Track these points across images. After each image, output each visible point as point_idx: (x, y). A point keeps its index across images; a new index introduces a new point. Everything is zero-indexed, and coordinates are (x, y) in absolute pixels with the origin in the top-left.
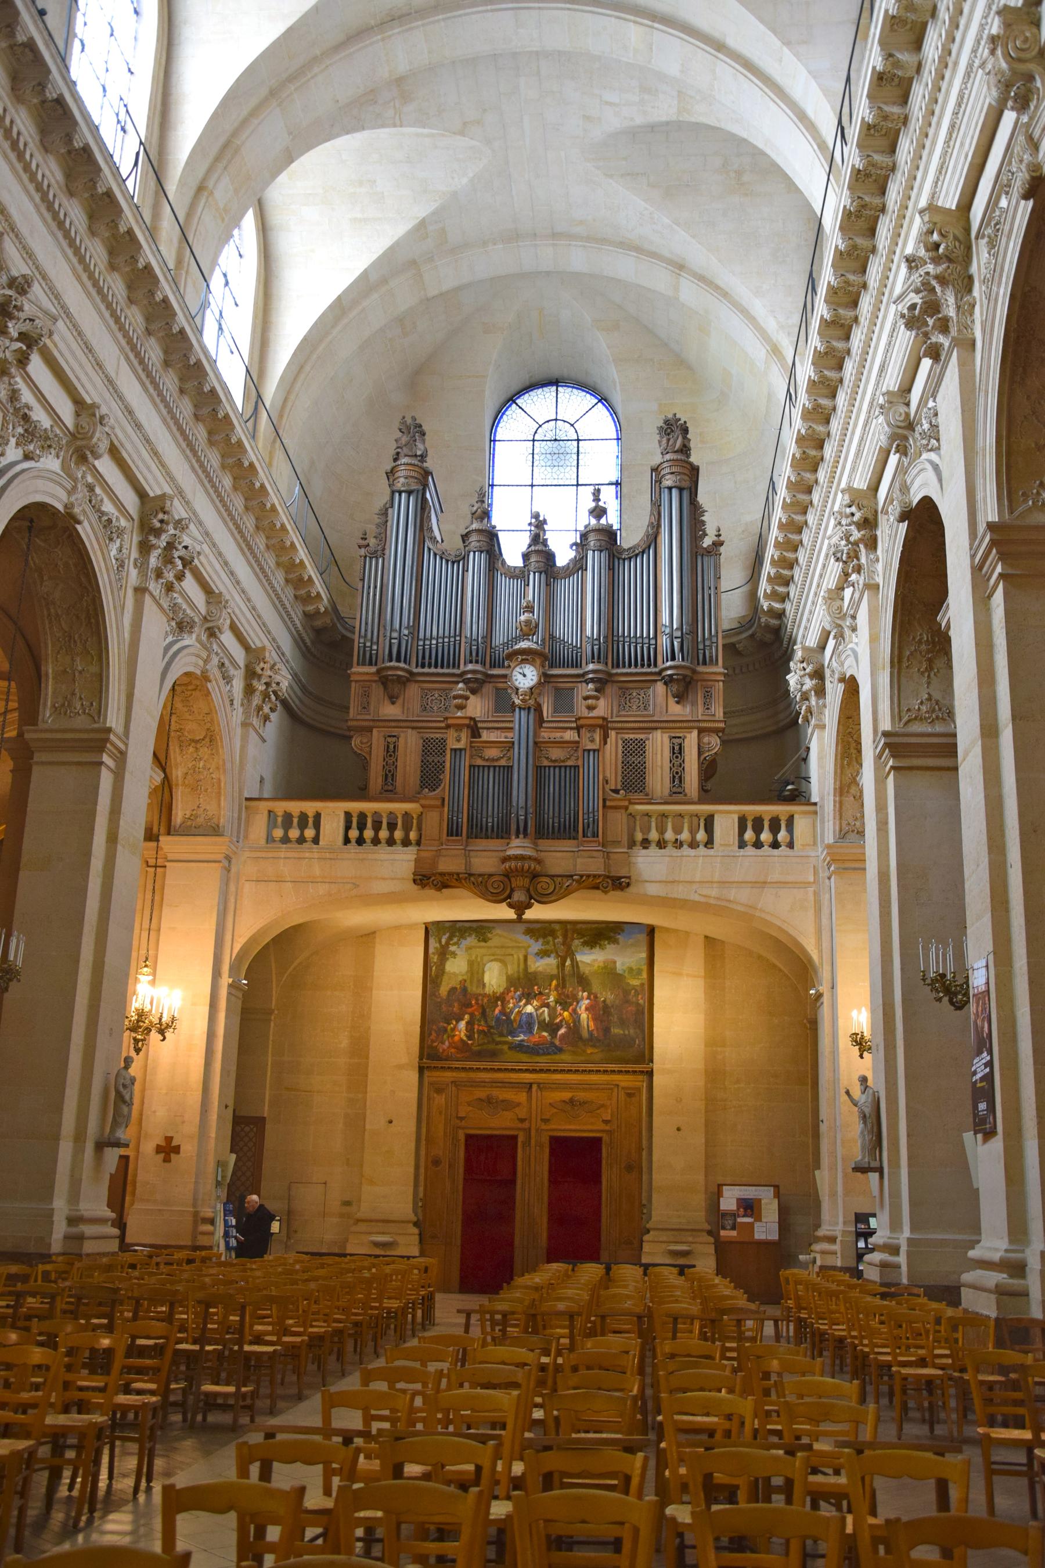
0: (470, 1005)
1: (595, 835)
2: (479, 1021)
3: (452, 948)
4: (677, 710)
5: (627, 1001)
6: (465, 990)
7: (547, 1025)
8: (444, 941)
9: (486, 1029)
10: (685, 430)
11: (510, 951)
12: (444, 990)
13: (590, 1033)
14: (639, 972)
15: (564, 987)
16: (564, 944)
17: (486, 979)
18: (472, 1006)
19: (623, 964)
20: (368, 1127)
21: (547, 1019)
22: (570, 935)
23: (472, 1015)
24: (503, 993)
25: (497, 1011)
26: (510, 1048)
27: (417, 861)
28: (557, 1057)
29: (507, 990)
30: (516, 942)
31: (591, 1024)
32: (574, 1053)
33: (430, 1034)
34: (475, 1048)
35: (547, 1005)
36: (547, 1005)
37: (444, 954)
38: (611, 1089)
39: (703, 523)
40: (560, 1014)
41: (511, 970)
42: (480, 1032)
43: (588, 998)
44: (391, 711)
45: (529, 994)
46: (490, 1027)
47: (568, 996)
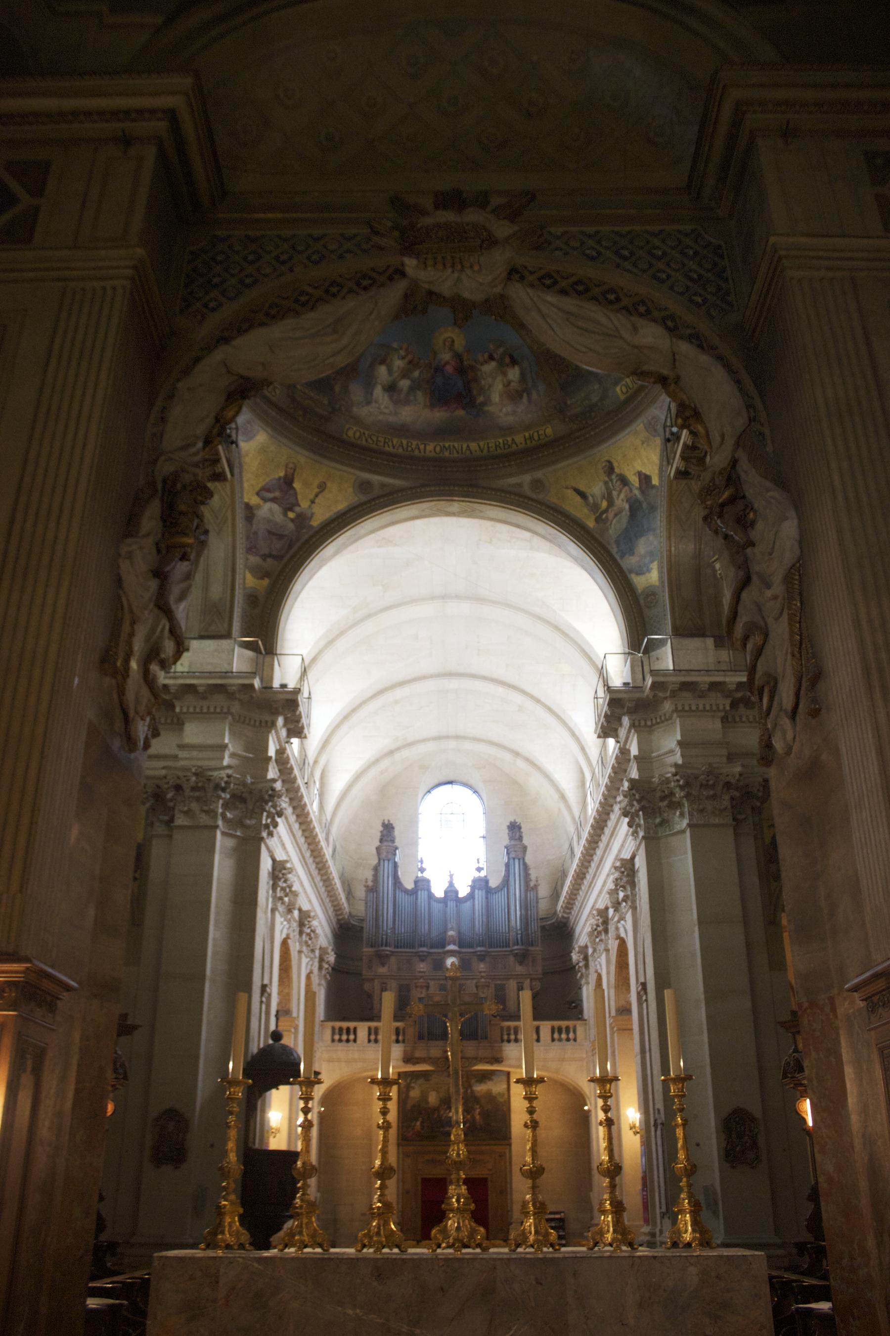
1: (486, 1038)
3: (413, 1085)
4: (520, 969)
10: (520, 828)
25: (435, 1116)
27: (405, 1052)
37: (408, 1088)
39: (529, 874)
44: (383, 970)
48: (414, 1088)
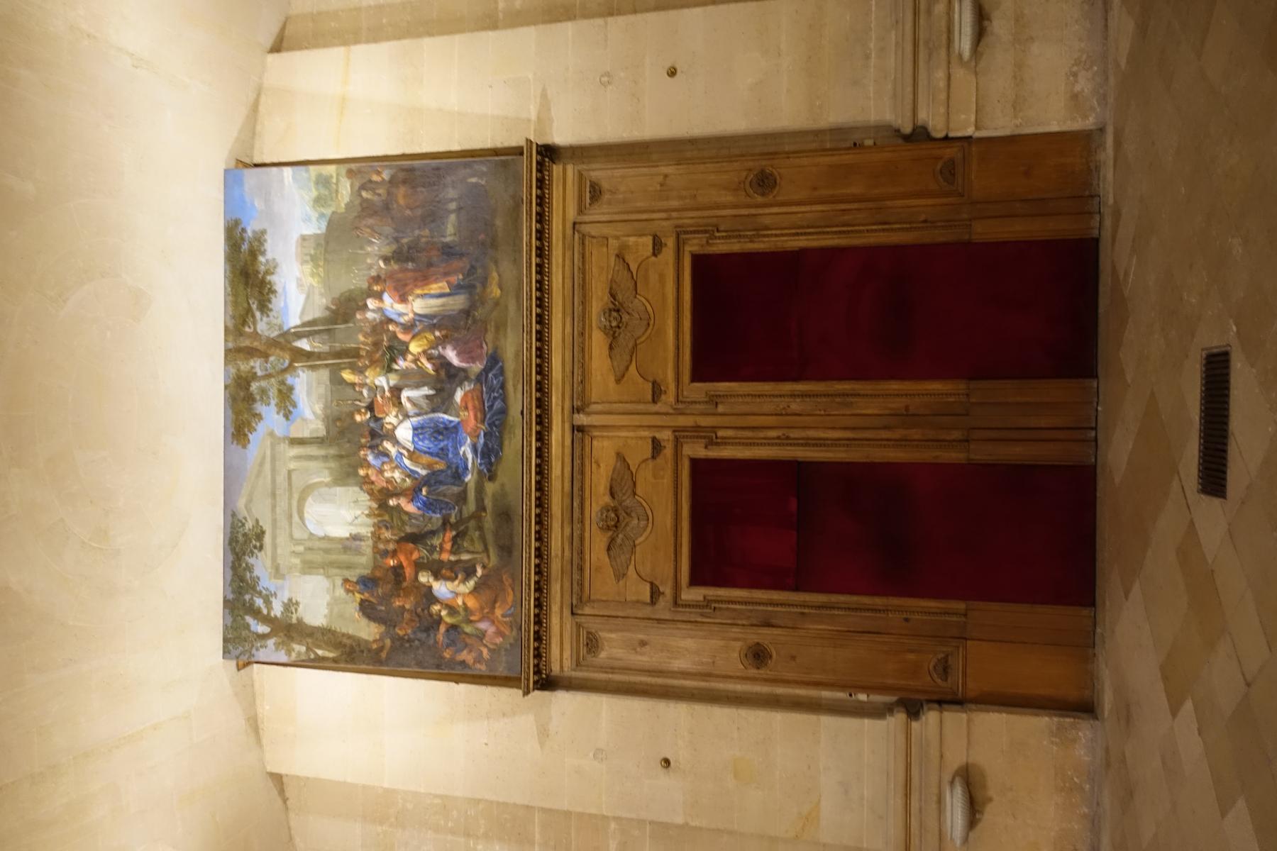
0: (398, 571)
2: (432, 549)
3: (277, 610)
5: (387, 207)
6: (367, 582)
7: (439, 391)
8: (262, 629)
9: (450, 534)
11: (281, 479)
12: (368, 631)
13: (456, 289)
14: (323, 182)
15: (354, 354)
16: (266, 356)
17: (342, 532)
18: (400, 566)
19: (307, 220)
20: (679, 820)
21: (426, 391)
22: (246, 343)
23: (419, 566)
24: (371, 493)
25: (410, 508)
26: (492, 478)
28: (510, 365)
29: (365, 482)
30: (261, 464)
31: (435, 288)
32: (500, 327)
33: (463, 663)
34: (494, 560)
35: (396, 391)
36: (396, 391)
37: (289, 629)
38: (583, 238)
40: (416, 361)
41: (320, 473)
42: (456, 549)
43: (379, 296)
45: (374, 434)
46: (445, 523)
47: (377, 344)
48: (290, 605)
